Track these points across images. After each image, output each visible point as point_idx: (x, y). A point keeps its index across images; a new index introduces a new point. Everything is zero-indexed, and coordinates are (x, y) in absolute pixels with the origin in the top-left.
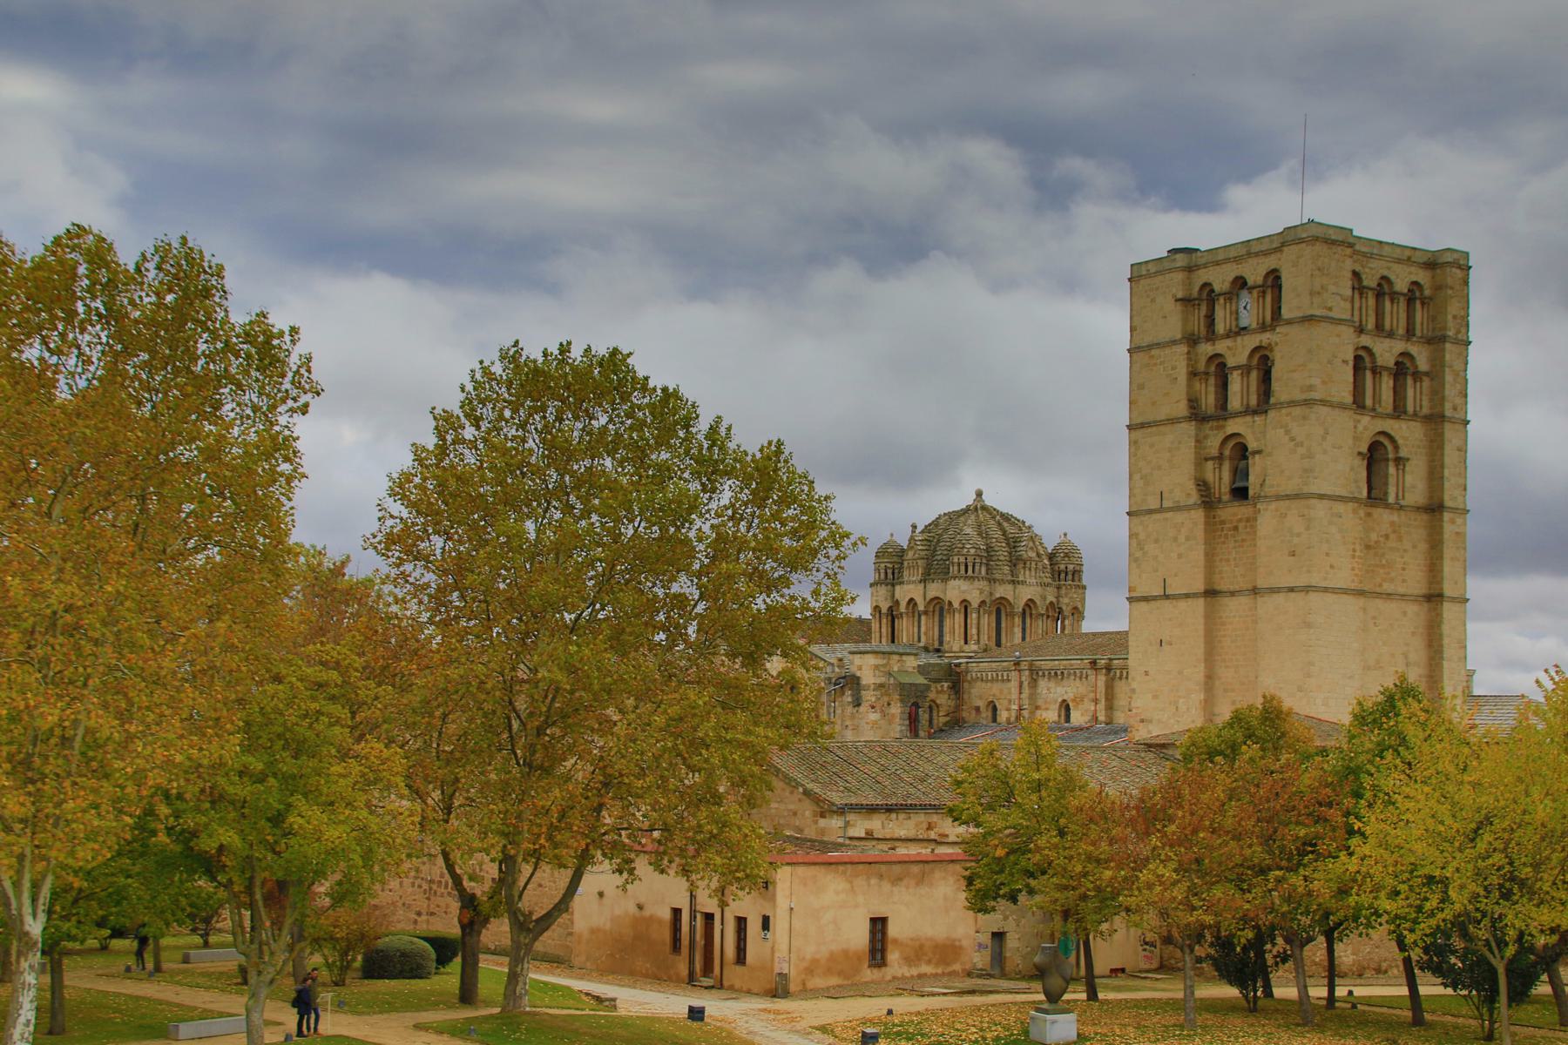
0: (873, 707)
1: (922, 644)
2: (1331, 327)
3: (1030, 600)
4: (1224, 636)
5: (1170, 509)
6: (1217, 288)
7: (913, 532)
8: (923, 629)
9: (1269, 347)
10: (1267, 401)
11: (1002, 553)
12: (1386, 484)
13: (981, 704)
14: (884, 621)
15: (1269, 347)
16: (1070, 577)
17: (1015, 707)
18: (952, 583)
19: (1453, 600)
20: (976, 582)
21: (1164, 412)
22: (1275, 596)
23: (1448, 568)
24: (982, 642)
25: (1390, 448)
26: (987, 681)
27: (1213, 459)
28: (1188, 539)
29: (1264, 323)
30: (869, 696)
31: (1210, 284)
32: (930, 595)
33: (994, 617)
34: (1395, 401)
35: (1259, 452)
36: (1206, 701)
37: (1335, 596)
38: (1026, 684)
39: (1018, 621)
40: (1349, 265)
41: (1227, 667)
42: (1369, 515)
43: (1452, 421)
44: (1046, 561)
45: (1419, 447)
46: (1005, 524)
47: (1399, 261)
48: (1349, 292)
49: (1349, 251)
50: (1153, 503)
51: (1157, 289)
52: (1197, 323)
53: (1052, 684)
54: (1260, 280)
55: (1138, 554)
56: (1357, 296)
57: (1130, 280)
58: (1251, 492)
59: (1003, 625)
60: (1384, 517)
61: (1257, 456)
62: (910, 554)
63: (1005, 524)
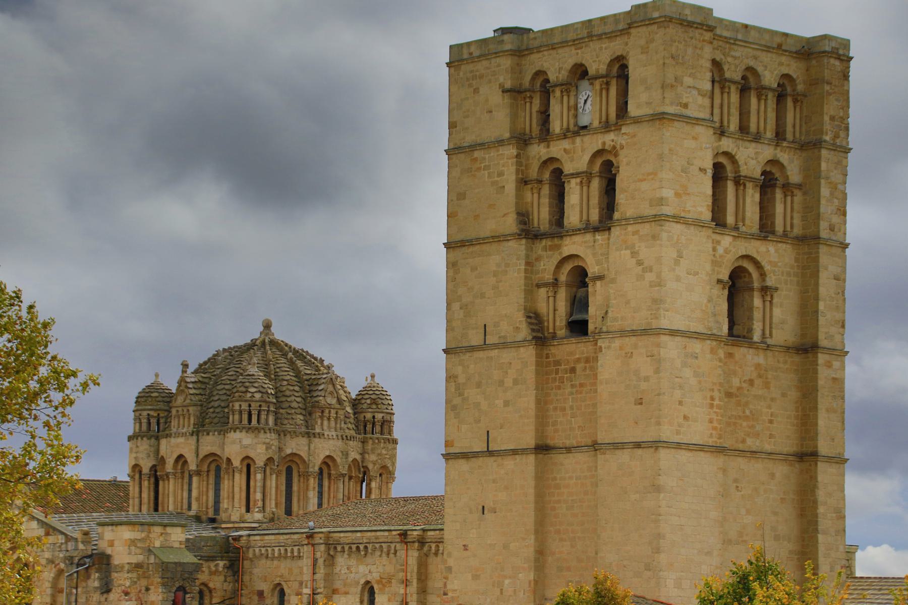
0: (127, 594)
1: (192, 513)
2: (687, 128)
3: (329, 457)
4: (559, 502)
5: (495, 346)
6: (552, 77)
7: (184, 372)
8: (195, 493)
9: (614, 151)
10: (610, 218)
11: (295, 400)
12: (751, 318)
13: (265, 587)
14: (145, 484)
15: (614, 151)
16: (378, 428)
17: (307, 591)
18: (233, 436)
19: (830, 459)
20: (262, 435)
21: (489, 227)
22: (617, 452)
23: (823, 421)
24: (268, 509)
25: (755, 275)
26: (273, 559)
27: (546, 285)
28: (516, 382)
29: (607, 121)
30: (122, 580)
31: (545, 73)
32: (205, 450)
33: (283, 479)
34: (761, 219)
35: (600, 278)
36: (536, 582)
37: (689, 454)
38: (321, 562)
39: (313, 482)
40: (708, 52)
41: (561, 540)
42: (730, 355)
43: (828, 243)
44: (349, 409)
45: (789, 274)
46: (299, 363)
47: (768, 49)
48: (708, 86)
49: (708, 36)
50: (476, 339)
51: (481, 77)
52: (529, 120)
53: (353, 562)
54: (603, 69)
55: (457, 401)
56: (717, 91)
57: (449, 65)
58: (591, 327)
59: (295, 488)
60: (748, 358)
61: (598, 283)
62: (180, 400)
63: (299, 363)
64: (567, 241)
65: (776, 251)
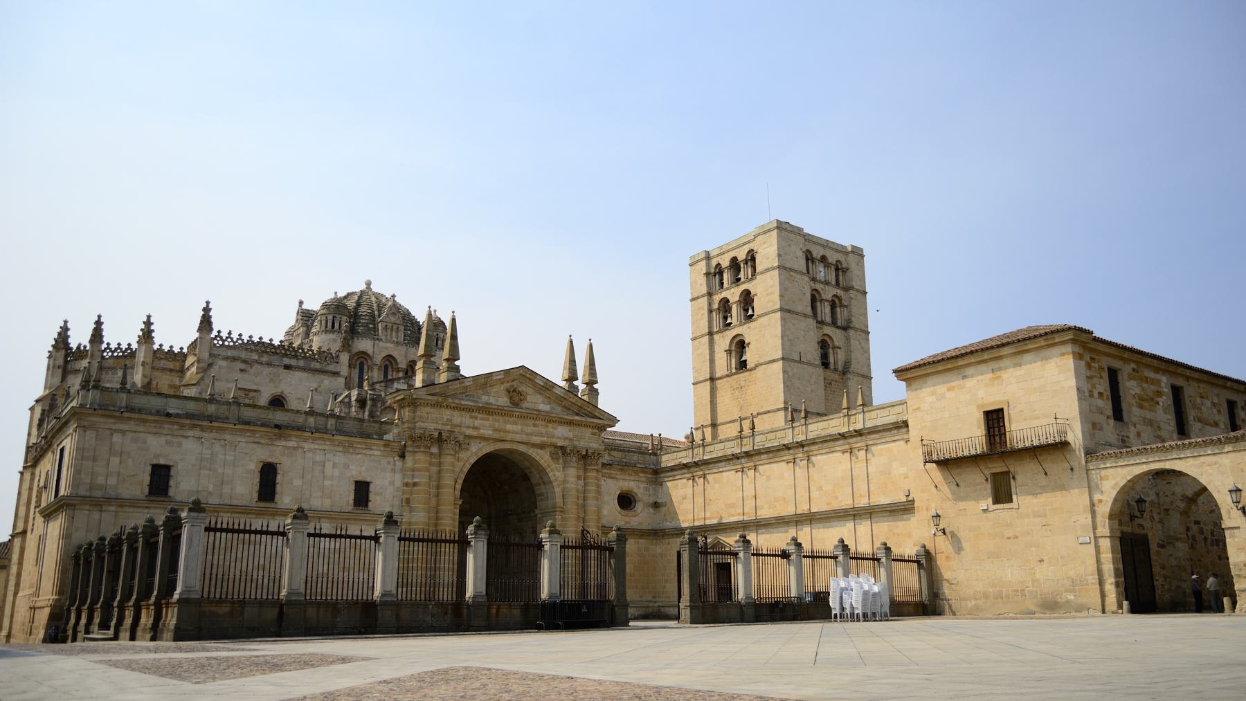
28: (816, 383)
55: (788, 383)
64: (825, 327)
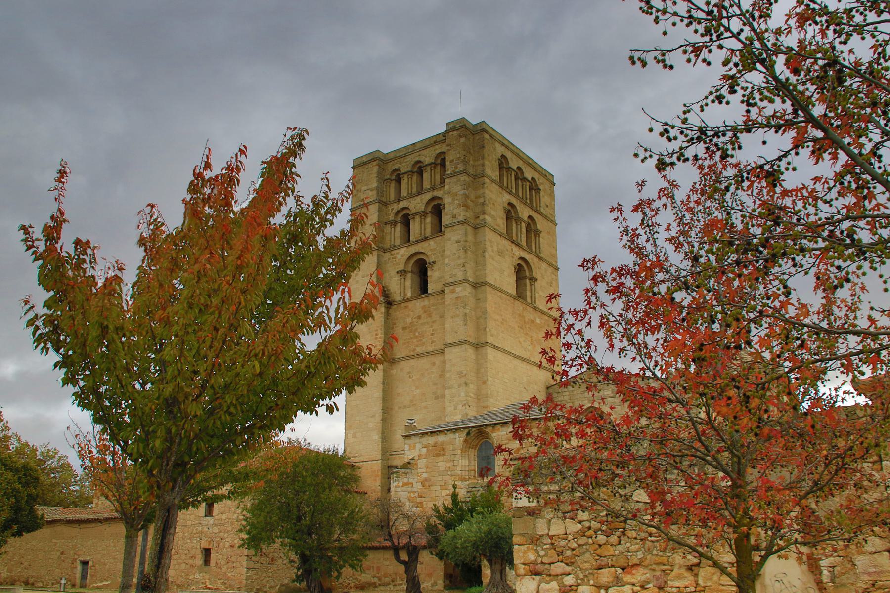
65: (435, 243)
